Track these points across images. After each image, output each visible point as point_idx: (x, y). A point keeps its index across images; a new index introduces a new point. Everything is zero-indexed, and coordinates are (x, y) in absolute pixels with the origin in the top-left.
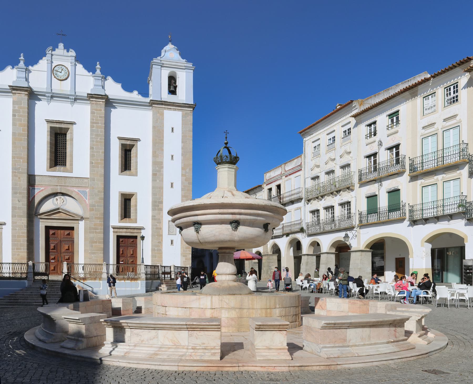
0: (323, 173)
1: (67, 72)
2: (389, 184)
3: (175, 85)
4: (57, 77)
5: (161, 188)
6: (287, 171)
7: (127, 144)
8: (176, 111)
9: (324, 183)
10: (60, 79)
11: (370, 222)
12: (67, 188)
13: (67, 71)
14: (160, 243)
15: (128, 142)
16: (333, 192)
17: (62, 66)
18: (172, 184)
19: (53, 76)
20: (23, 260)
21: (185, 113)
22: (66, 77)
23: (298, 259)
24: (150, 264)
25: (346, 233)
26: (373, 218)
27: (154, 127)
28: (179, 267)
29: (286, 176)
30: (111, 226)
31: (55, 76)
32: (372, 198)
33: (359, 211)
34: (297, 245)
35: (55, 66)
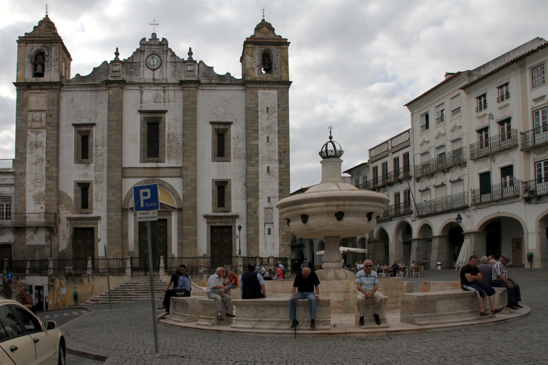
0: (433, 149)
1: (160, 61)
2: (503, 161)
3: (269, 63)
4: (149, 67)
5: (257, 174)
6: (394, 147)
7: (220, 129)
8: (271, 90)
9: (434, 160)
10: (153, 68)
11: (483, 201)
12: (161, 179)
13: (159, 59)
14: (257, 233)
15: (222, 127)
16: (444, 170)
17: (155, 55)
18: (268, 168)
19: (146, 67)
20: (118, 256)
21: (280, 91)
22: (159, 66)
23: (407, 244)
24: (246, 256)
25: (459, 214)
26: (486, 198)
27: (247, 109)
28: (278, 258)
29: (393, 153)
30: (206, 217)
31: (148, 65)
32: (485, 177)
33: (471, 189)
34: (406, 229)
35: (148, 57)
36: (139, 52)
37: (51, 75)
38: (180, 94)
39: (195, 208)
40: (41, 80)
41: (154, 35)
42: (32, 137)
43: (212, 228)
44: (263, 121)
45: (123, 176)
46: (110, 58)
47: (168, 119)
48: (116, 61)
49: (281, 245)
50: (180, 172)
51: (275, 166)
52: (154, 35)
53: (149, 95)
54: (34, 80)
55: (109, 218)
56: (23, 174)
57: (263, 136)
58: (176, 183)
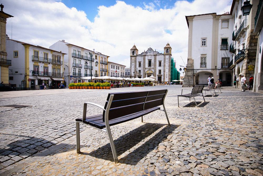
36: (148, 50)
37: (135, 55)
38: (154, 57)
39: (156, 74)
40: (134, 55)
41: (150, 48)
42: (132, 64)
43: (158, 77)
44: (166, 60)
45: (145, 69)
46: (144, 52)
47: (152, 60)
48: (144, 52)
49: (169, 80)
50: (153, 68)
51: (168, 68)
52: (150, 48)
53: (149, 57)
54: (133, 55)
55: (143, 75)
56: (131, 69)
57: (166, 63)
58: (153, 70)
